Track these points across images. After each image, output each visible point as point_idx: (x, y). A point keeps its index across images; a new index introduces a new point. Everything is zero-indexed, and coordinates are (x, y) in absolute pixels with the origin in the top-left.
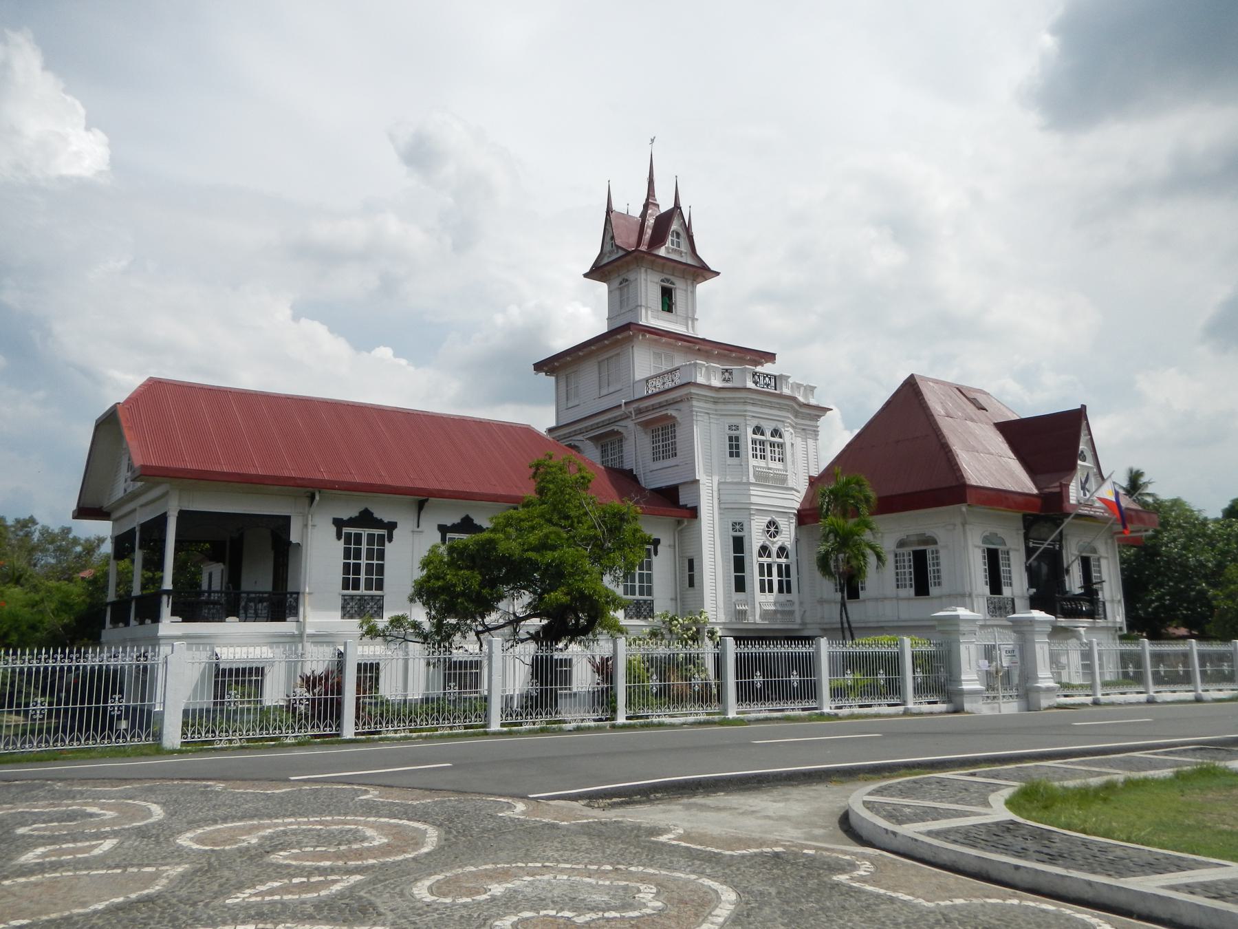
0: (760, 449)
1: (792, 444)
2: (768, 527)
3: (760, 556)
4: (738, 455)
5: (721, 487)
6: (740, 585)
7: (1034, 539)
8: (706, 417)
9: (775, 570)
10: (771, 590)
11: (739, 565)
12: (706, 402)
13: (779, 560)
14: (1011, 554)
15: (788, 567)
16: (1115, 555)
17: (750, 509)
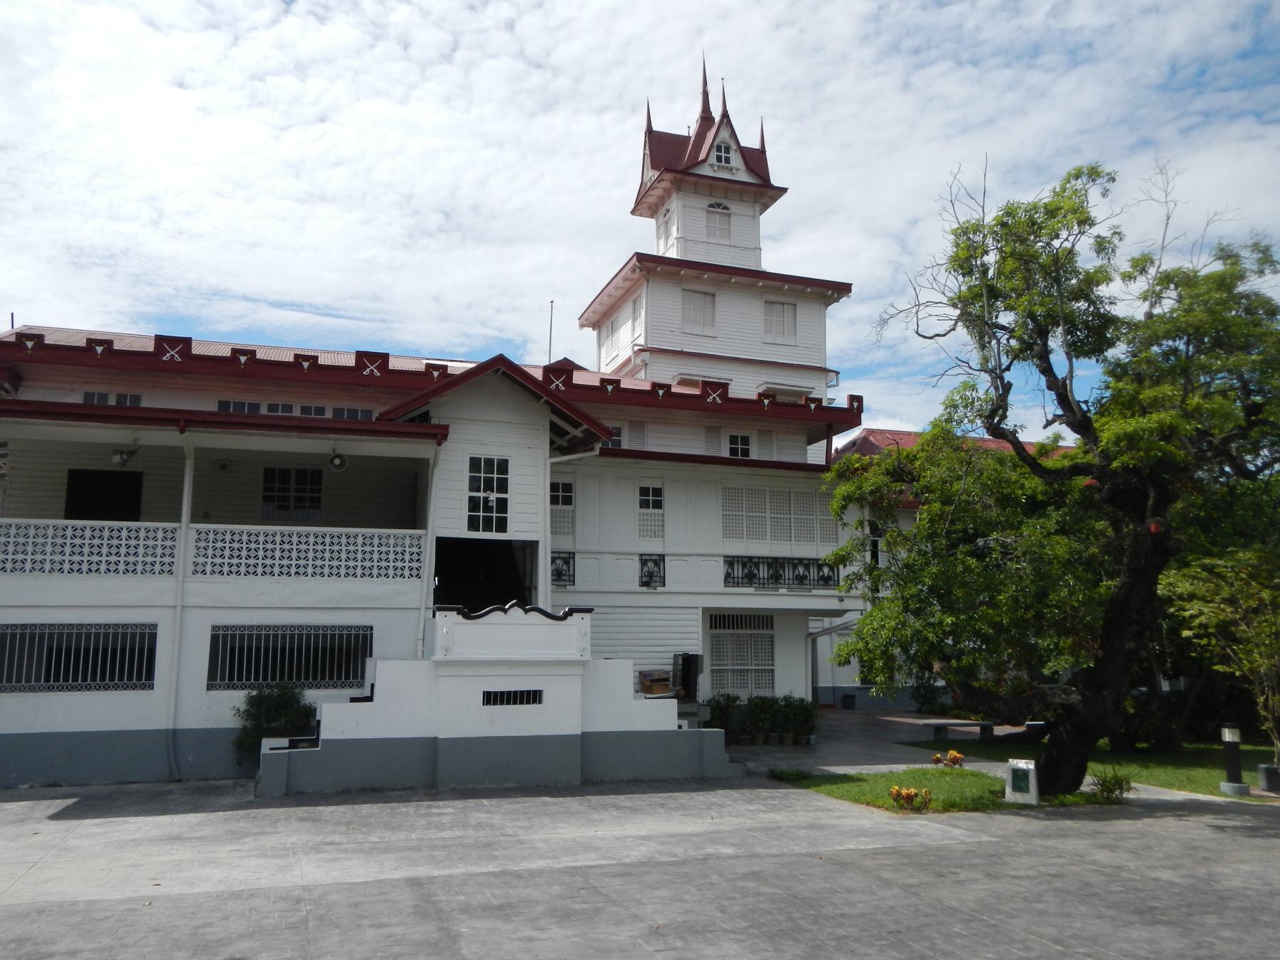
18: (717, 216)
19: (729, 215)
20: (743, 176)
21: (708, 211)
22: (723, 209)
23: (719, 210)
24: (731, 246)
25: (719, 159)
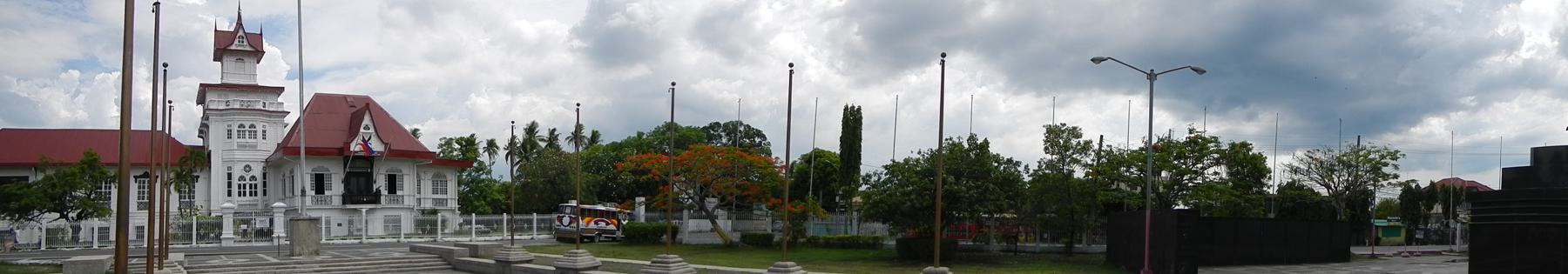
0: (241, 134)
1: (264, 132)
6: (230, 194)
9: (248, 187)
10: (245, 195)
11: (230, 185)
14: (333, 176)
15: (256, 185)
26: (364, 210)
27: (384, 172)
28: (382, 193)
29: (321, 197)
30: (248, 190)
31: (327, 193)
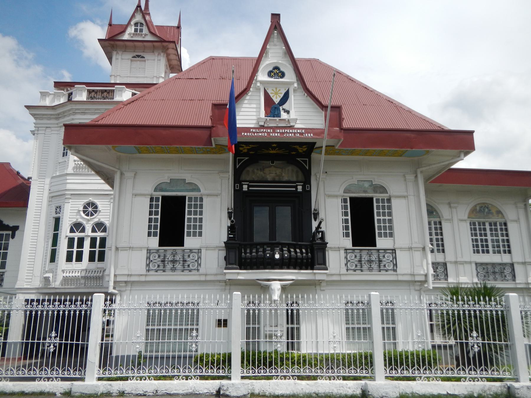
2: (85, 207)
3: (72, 231)
4: (66, 155)
5: (54, 180)
6: (53, 258)
7: (250, 182)
8: (48, 130)
9: (87, 243)
10: (79, 258)
12: (49, 119)
13: (94, 234)
16: (419, 196)
17: (64, 195)
18: (139, 62)
19: (145, 61)
20: (149, 38)
21: (131, 61)
22: (141, 58)
23: (139, 59)
24: (144, 77)
25: (136, 30)
26: (276, 286)
27: (341, 192)
28: (328, 239)
29: (174, 254)
30: (86, 249)
31: (189, 242)
